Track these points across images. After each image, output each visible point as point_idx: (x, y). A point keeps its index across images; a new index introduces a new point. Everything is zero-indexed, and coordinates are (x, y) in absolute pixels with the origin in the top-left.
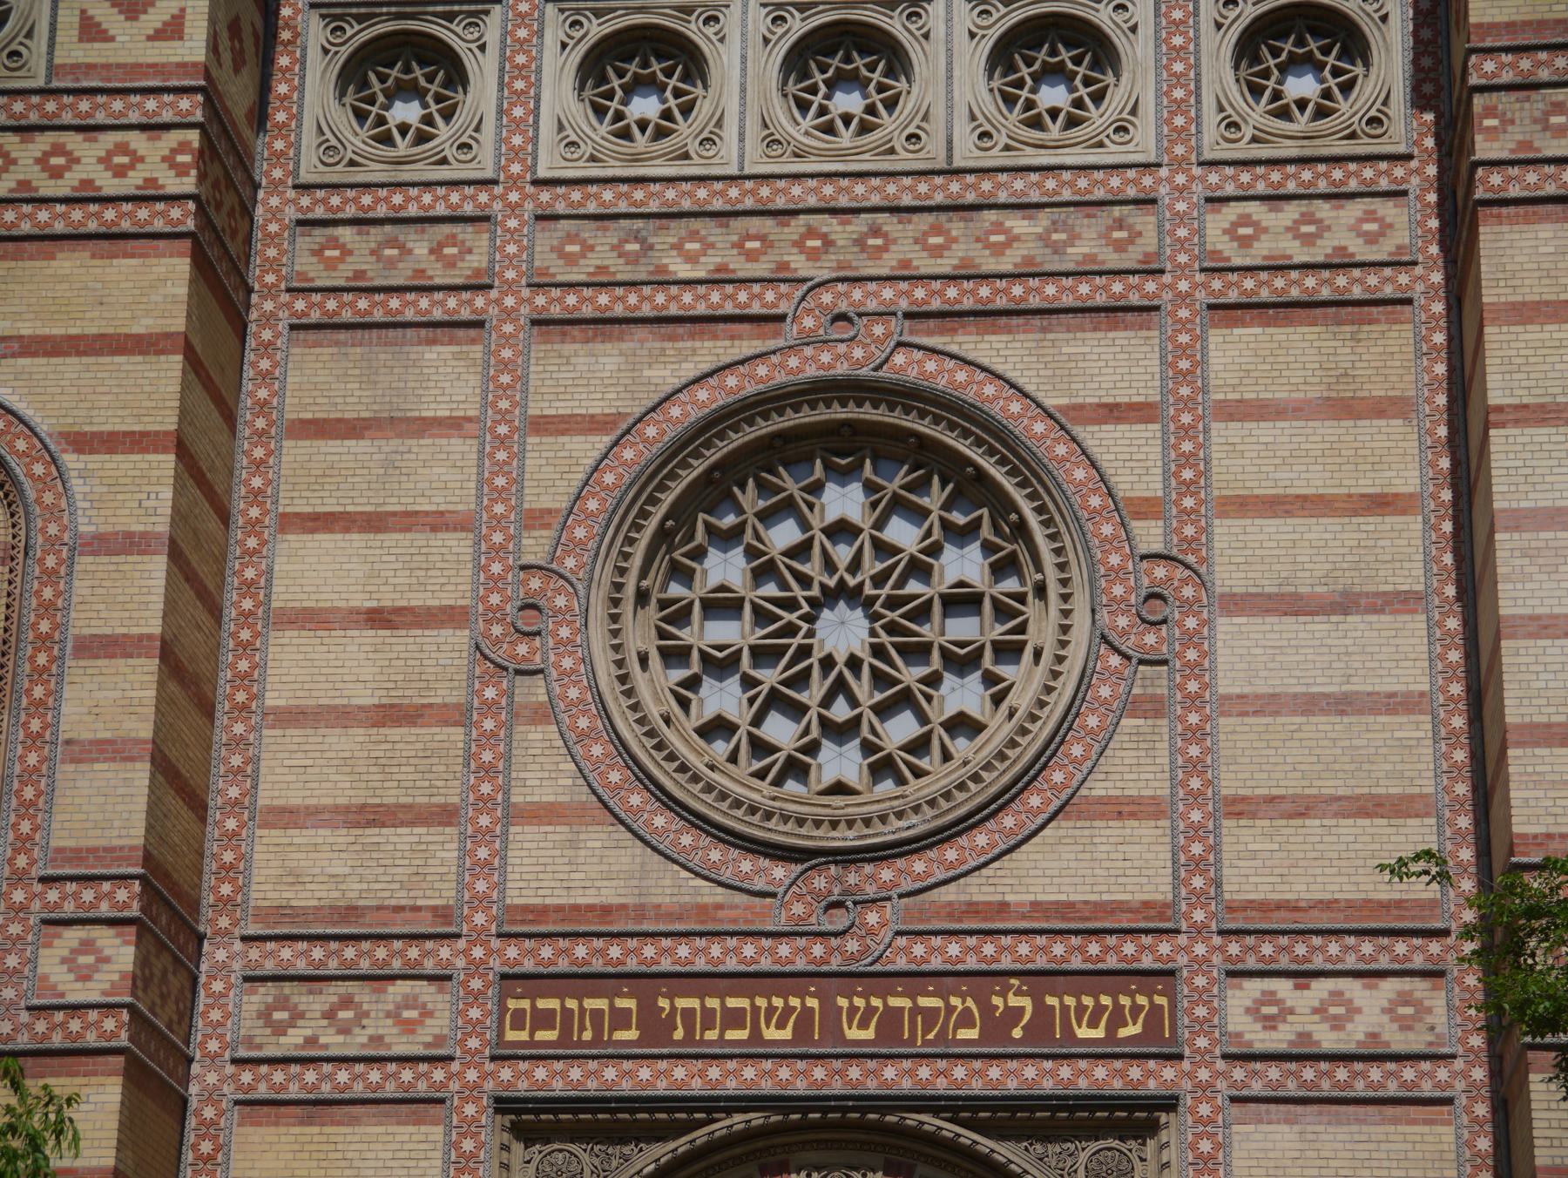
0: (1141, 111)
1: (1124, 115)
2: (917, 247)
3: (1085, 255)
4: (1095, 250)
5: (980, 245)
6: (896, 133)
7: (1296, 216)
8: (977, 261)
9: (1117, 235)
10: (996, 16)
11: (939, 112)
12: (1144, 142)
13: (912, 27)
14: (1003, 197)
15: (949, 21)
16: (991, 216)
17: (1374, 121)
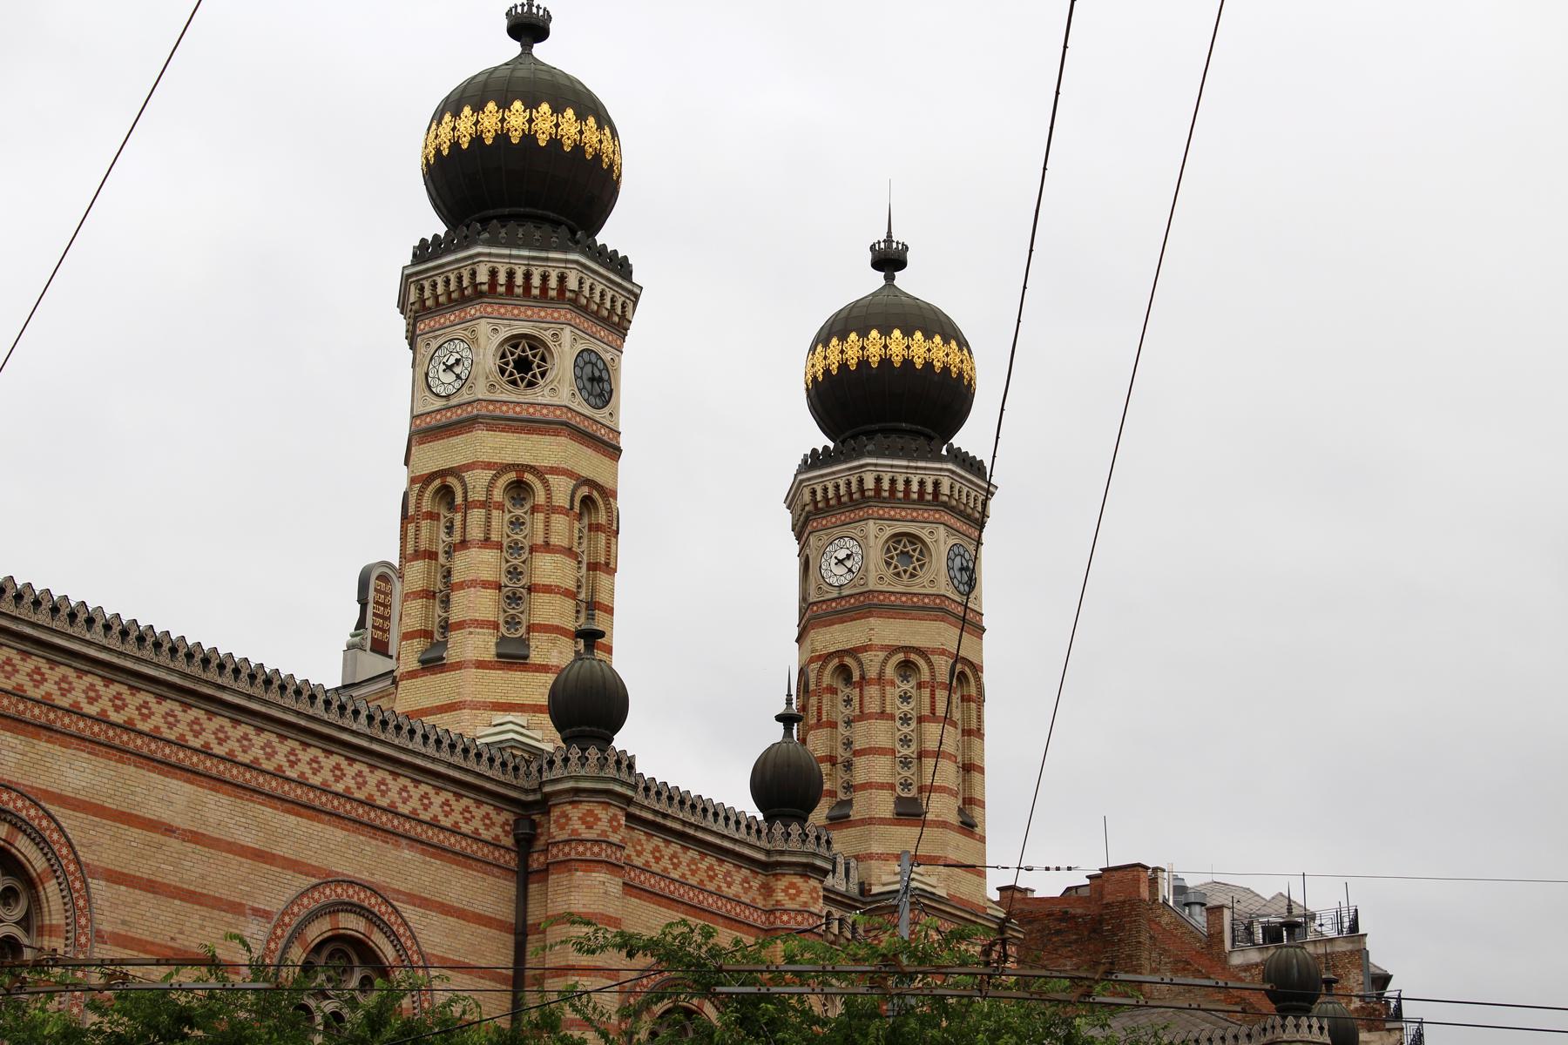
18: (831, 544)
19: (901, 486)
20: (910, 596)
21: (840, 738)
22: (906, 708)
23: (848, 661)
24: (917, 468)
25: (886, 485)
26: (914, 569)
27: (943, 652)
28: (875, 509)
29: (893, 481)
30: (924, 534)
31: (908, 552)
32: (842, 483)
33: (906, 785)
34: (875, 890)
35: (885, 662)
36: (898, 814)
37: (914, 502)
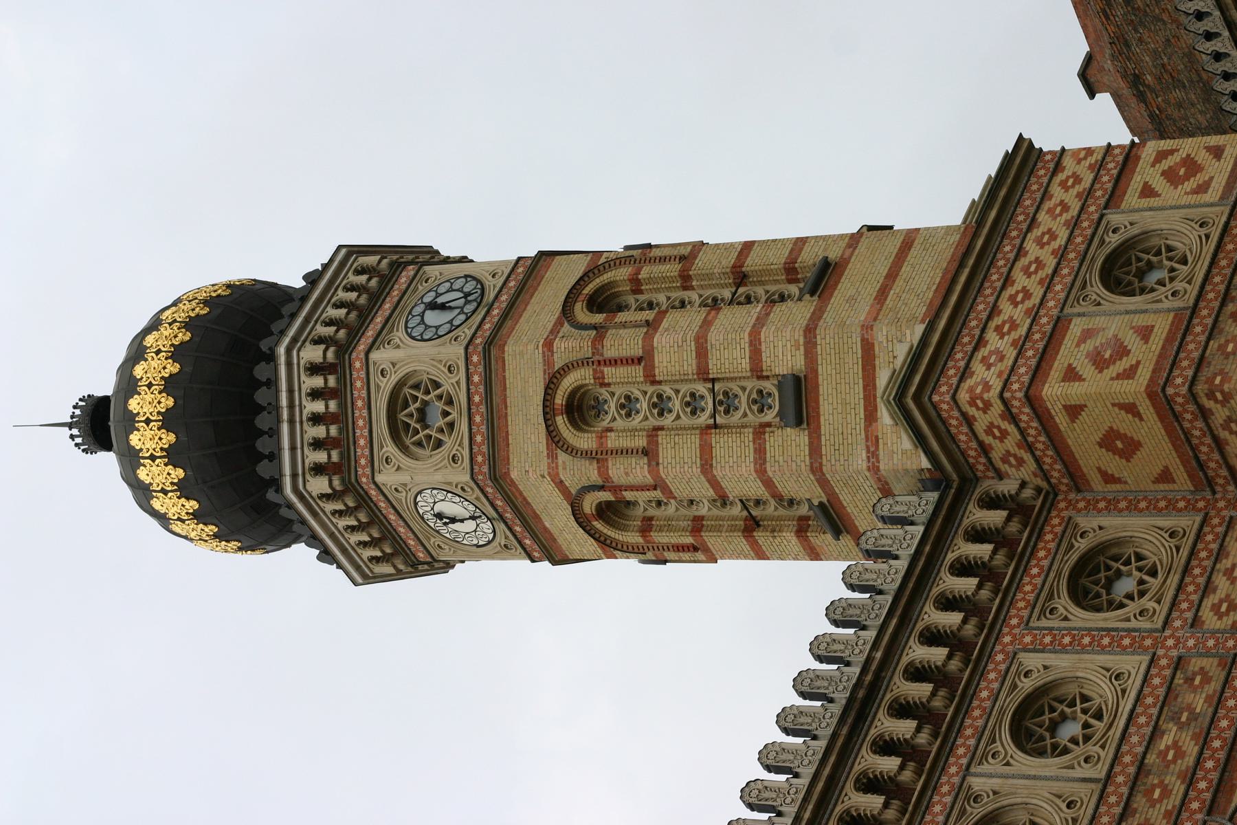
0: (1108, 665)
1: (1108, 675)
2: (1158, 806)
3: (1205, 702)
4: (1204, 695)
5: (1172, 766)
6: (1062, 815)
7: (1225, 578)
8: (1183, 768)
9: (1197, 681)
10: (1000, 749)
11: (1057, 786)
12: (1134, 664)
13: (985, 800)
14: (1140, 750)
15: (991, 776)
16: (1151, 759)
17: (1171, 536)
18: (438, 532)
19: (320, 431)
20: (474, 410)
21: (715, 512)
22: (643, 405)
23: (589, 504)
24: (291, 406)
25: (321, 457)
26: (440, 397)
27: (549, 344)
28: (360, 471)
29: (317, 444)
30: (386, 385)
31: (418, 410)
32: (342, 523)
33: (760, 401)
34: (925, 463)
35: (571, 451)
36: (799, 422)
37: (342, 405)
